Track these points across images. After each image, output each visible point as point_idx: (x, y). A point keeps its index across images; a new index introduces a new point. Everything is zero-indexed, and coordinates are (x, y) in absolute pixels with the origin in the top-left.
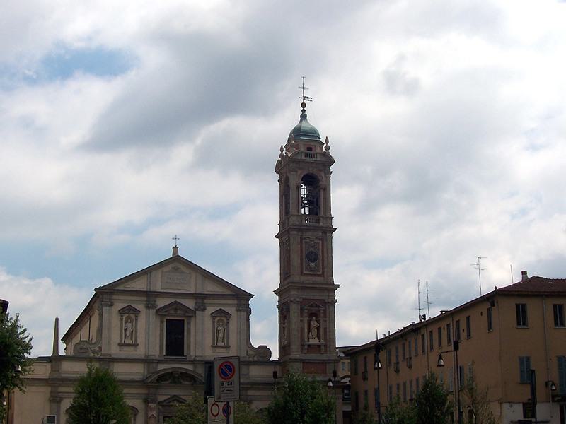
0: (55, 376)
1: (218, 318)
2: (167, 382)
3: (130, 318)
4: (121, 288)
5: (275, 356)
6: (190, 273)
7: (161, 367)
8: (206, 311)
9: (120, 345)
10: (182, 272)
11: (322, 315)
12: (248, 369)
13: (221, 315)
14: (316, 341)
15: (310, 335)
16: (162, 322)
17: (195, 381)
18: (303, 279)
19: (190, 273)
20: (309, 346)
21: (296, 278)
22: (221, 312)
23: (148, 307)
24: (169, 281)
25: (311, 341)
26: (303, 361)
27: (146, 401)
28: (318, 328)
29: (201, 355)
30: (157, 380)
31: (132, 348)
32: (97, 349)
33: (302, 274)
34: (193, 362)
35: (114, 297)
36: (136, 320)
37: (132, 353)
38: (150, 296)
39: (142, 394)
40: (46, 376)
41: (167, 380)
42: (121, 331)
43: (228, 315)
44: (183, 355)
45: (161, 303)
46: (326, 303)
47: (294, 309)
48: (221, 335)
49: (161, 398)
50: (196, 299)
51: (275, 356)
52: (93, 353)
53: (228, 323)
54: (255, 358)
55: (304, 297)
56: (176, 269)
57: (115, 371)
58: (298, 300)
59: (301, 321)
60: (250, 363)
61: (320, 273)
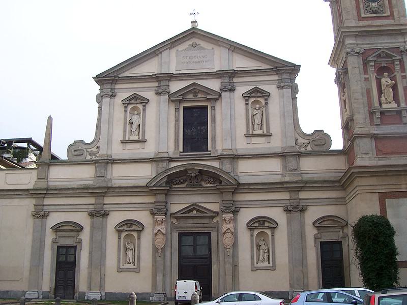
0: (42, 184)
1: (253, 100)
2: (184, 185)
4: (126, 74)
5: (337, 144)
6: (213, 49)
7: (173, 165)
8: (236, 92)
9: (124, 142)
10: (202, 48)
11: (397, 68)
12: (298, 163)
13: (257, 95)
14: (394, 105)
15: (383, 99)
16: (177, 110)
17: (221, 182)
18: (362, 23)
20: (382, 113)
21: (351, 22)
22: (256, 91)
23: (158, 94)
24: (186, 60)
25: (384, 106)
26: (375, 137)
27: (153, 214)
28: (395, 87)
30: (167, 183)
31: (137, 146)
33: (360, 18)
34: (219, 158)
35: (117, 86)
37: (137, 151)
38: (162, 79)
39: (149, 203)
40: (31, 187)
41: (182, 183)
42: (125, 123)
43: (266, 95)
45: (176, 86)
46: (402, 51)
47: (354, 63)
48: (257, 120)
49: (175, 208)
50: (220, 78)
51: (337, 144)
52: (90, 154)
53: (266, 104)
54: (309, 148)
55: (367, 47)
56: (194, 45)
57: (114, 175)
58: (357, 50)
59: (366, 79)
60: (300, 155)
61: (388, 14)
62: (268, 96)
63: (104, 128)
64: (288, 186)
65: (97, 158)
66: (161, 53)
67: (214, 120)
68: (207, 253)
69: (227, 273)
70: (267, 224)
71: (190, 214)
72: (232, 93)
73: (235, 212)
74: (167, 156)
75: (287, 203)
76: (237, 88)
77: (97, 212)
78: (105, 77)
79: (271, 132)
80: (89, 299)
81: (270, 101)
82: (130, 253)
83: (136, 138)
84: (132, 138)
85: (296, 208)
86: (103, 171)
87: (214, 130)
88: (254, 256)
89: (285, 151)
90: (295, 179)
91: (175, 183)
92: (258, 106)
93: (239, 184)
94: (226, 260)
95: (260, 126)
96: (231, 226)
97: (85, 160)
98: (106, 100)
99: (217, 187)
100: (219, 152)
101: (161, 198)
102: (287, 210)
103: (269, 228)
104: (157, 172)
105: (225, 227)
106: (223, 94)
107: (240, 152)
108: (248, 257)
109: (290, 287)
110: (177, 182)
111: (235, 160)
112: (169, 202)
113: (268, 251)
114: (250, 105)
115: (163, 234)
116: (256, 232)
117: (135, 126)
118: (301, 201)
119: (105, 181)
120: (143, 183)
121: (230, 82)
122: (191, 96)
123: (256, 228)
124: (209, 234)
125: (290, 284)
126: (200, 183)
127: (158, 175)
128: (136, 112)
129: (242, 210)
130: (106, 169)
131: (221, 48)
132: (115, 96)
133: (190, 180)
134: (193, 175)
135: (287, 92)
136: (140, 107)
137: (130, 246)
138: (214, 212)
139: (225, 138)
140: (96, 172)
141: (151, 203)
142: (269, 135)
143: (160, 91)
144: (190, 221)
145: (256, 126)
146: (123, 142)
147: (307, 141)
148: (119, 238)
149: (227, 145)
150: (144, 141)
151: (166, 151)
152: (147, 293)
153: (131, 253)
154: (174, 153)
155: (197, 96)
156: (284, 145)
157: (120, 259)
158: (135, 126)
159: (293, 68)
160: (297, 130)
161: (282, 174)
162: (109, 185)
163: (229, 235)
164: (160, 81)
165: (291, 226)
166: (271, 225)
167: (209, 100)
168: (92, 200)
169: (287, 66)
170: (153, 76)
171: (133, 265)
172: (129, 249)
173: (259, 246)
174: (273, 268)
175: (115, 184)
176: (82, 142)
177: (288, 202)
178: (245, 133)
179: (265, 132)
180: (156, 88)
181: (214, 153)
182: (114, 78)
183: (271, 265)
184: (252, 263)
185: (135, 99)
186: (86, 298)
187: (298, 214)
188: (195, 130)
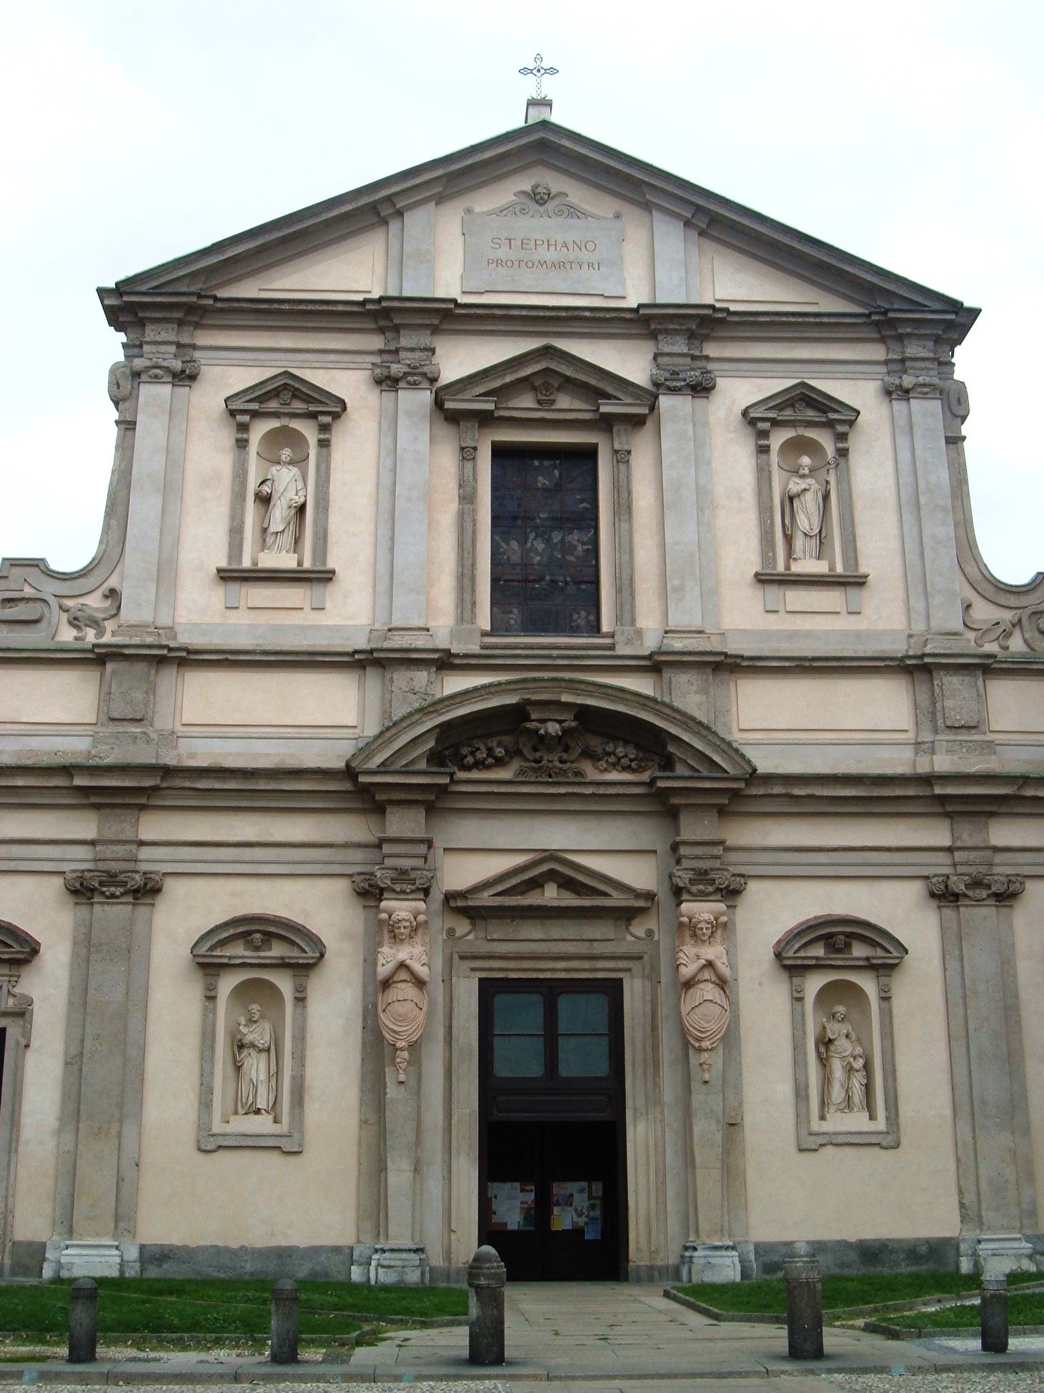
1: (786, 434)
3: (294, 439)
7: (456, 683)
10: (574, 212)
12: (982, 698)
16: (467, 454)
17: (668, 763)
19: (618, 216)
23: (387, 382)
24: (503, 253)
27: (370, 893)
29: (697, 623)
30: (436, 758)
32: (95, 602)
34: (655, 665)
35: (204, 338)
36: (324, 444)
39: (347, 845)
41: (500, 763)
44: (595, 628)
48: (807, 519)
50: (653, 336)
52: (74, 622)
53: (843, 453)
54: (1016, 644)
56: (539, 198)
60: (987, 668)
62: (851, 423)
63: (143, 507)
64: (950, 790)
65: (108, 638)
66: (400, 214)
67: (624, 507)
68: (601, 1068)
69: (698, 1160)
70: (859, 951)
71: (532, 899)
72: (700, 402)
73: (731, 894)
74: (429, 645)
75: (940, 865)
76: (721, 382)
77: (112, 878)
78: (154, 292)
79: (863, 569)
80: (65, 1274)
81: (856, 444)
82: (256, 1067)
83: (287, 561)
84: (270, 560)
85: (977, 883)
86: (138, 695)
87: (625, 549)
88: (807, 1086)
89: (928, 650)
90: (976, 765)
91: (470, 759)
92: (806, 460)
93: (753, 777)
94: (697, 1099)
95: (814, 543)
96: (713, 952)
97: (51, 646)
98: (154, 395)
99: (661, 784)
100: (650, 643)
101: (403, 823)
102: (944, 896)
103: (871, 967)
104: (386, 713)
105: (691, 958)
106: (665, 402)
107: (735, 647)
108: (784, 1090)
109: (964, 1219)
110: (481, 755)
111: (725, 676)
112: (439, 844)
113: (867, 1067)
114: (774, 457)
115: (420, 983)
116: (814, 984)
117: (279, 515)
118: (999, 858)
119: (148, 741)
120: (332, 755)
121: (694, 358)
122: (525, 403)
123: (819, 966)
124: (613, 990)
125: (962, 1205)
126: (574, 765)
127: (389, 730)
128: (286, 453)
129: (753, 886)
130: (152, 690)
131: (654, 213)
132: (193, 378)
133: (535, 749)
134: (553, 728)
135: (927, 411)
136: (308, 431)
137: (260, 1034)
138: (637, 894)
139: (677, 582)
140: (105, 697)
141: (360, 846)
142: (853, 582)
143: (396, 369)
144: (532, 930)
145: (799, 542)
146: (227, 576)
147: (1008, 616)
148: (211, 998)
149: (686, 614)
150: (321, 577)
151: (421, 624)
152: (336, 1250)
153: (263, 1067)
154: (453, 634)
155: (553, 402)
156: (919, 627)
157: (211, 1091)
158: (279, 515)
159: (952, 317)
160: (968, 569)
161: (917, 744)
162: (169, 759)
163: (708, 991)
164: (397, 329)
165: (961, 959)
166: (880, 953)
167: (606, 423)
168: (83, 826)
169: (920, 307)
170: (369, 307)
171: (271, 1118)
172: (253, 1045)
173: (825, 1043)
174: (889, 1140)
175: (192, 756)
176: (37, 564)
177: (942, 858)
178: (757, 568)
179: (839, 569)
180: (377, 359)
181: (629, 642)
182: (194, 299)
183: (881, 1125)
184: (801, 1117)
185: (286, 396)
186: (48, 1272)
187: (981, 916)
188: (540, 546)
